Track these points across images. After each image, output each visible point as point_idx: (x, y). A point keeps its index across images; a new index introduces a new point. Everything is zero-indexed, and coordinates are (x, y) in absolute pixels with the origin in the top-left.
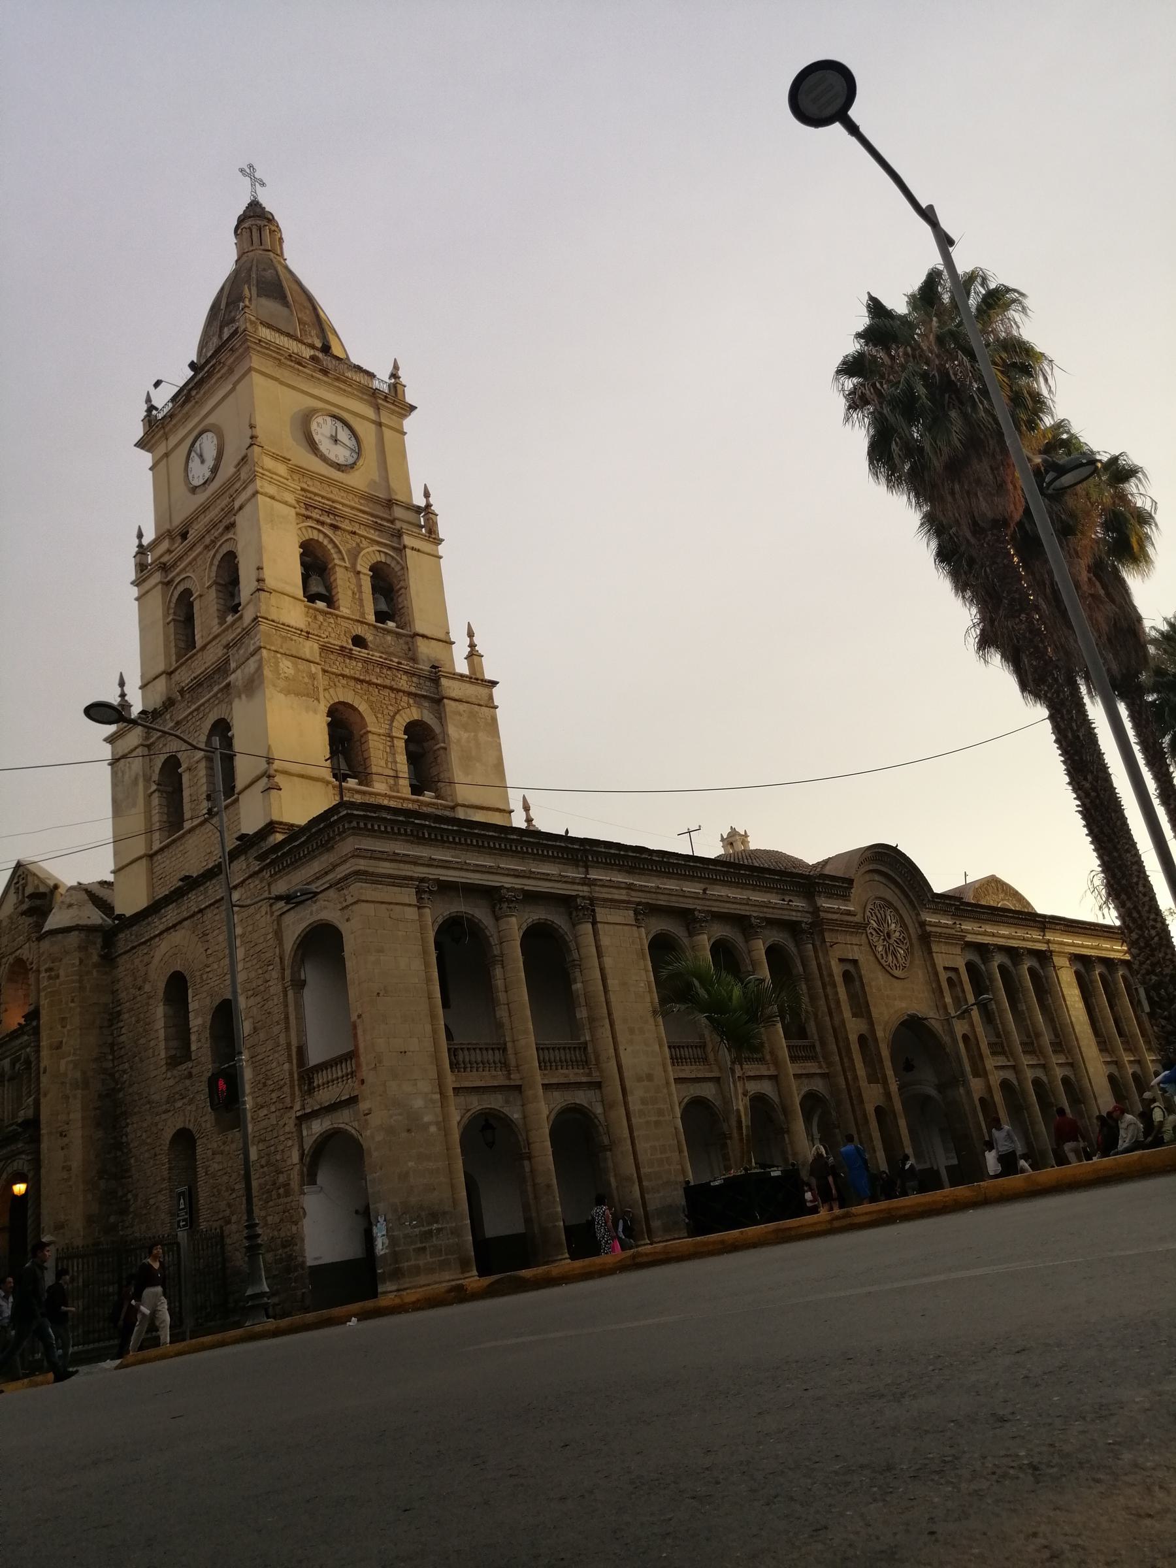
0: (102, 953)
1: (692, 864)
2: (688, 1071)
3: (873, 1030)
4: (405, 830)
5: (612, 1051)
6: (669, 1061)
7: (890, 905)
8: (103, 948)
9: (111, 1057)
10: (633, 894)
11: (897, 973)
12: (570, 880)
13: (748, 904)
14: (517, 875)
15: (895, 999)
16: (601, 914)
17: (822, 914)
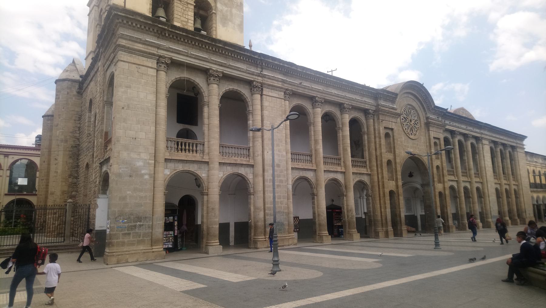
0: (77, 91)
1: (318, 75)
2: (300, 165)
3: (395, 159)
4: (153, 30)
5: (260, 152)
6: (290, 160)
7: (413, 108)
8: (78, 89)
9: (78, 132)
10: (285, 85)
11: (411, 137)
12: (251, 73)
13: (344, 98)
14: (221, 65)
15: (408, 148)
16: (266, 91)
17: (380, 107)
